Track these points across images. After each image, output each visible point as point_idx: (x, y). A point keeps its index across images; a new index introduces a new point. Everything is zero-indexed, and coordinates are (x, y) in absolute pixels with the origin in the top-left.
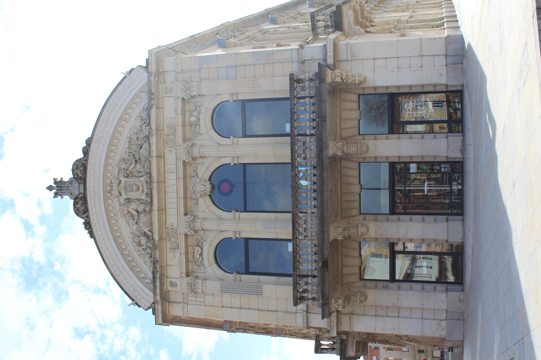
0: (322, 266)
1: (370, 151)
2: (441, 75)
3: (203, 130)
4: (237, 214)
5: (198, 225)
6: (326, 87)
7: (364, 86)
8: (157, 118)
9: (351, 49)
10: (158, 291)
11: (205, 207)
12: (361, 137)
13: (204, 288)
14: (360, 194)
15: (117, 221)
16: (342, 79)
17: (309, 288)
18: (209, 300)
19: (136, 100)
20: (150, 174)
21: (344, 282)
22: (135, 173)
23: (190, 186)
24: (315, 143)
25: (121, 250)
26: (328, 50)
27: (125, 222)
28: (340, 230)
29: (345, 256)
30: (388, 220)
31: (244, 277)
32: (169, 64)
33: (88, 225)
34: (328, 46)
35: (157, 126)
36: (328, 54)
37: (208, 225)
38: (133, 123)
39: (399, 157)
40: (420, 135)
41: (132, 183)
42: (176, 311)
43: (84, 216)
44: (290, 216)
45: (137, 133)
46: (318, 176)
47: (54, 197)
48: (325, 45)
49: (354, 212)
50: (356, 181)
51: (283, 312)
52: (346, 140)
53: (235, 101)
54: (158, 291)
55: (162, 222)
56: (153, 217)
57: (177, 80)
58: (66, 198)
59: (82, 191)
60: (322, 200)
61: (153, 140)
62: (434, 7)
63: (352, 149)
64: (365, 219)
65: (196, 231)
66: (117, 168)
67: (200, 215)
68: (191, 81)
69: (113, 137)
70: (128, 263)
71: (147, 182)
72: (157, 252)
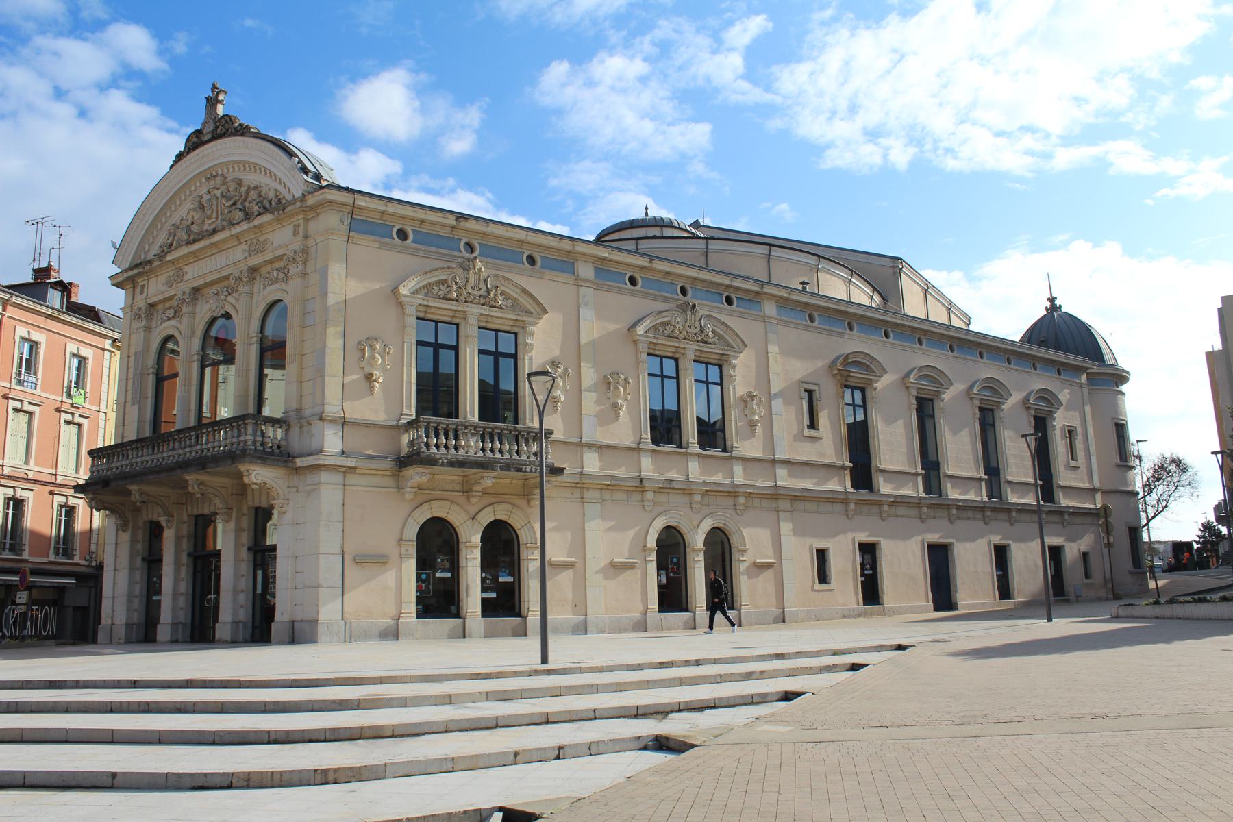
33: (180, 157)
67: (198, 309)
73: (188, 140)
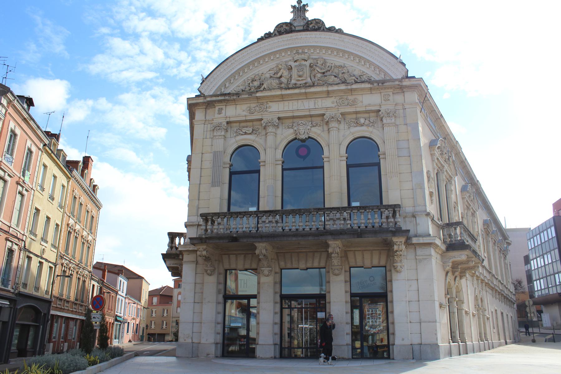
0: (233, 237)
1: (335, 277)
2: (403, 339)
3: (353, 129)
4: (281, 162)
5: (270, 129)
6: (389, 237)
7: (393, 271)
8: (362, 89)
9: (426, 259)
10: (214, 99)
11: (285, 135)
12: (348, 269)
13: (217, 137)
14: (298, 269)
15: (273, 60)
16: (396, 251)
17: (215, 227)
18: (208, 142)
19: (378, 70)
20: (313, 85)
21: (223, 256)
22: (313, 73)
23: (303, 121)
24: (338, 229)
25: (248, 65)
26: (425, 238)
27: (272, 67)
28: (264, 252)
29: (245, 257)
30: (276, 293)
31: (228, 170)
32: (413, 97)
33: (268, 36)
34: (428, 238)
35: (355, 90)
36: (421, 238)
37: (270, 138)
38: (357, 68)
39: (330, 303)
40: (350, 321)
41: (305, 70)
42: (199, 115)
43: (276, 31)
44: (279, 208)
45: (348, 72)
46: (310, 232)
47: (292, 6)
48: (429, 235)
49: (282, 264)
50: (309, 265)
51: (198, 205)
52: (345, 256)
53: (379, 156)
54: (214, 99)
55: (272, 99)
56: (276, 90)
57: (396, 105)
58: (291, 16)
59: (297, 29)
60: (289, 236)
61: (343, 87)
62: (480, 333)
63: (336, 261)
64: (276, 273)
65: (265, 128)
66: (317, 57)
67: (279, 131)
68: (395, 117)
69: (344, 52)
70: (238, 72)
71: (306, 83)
72: (247, 96)
73: (277, 27)
